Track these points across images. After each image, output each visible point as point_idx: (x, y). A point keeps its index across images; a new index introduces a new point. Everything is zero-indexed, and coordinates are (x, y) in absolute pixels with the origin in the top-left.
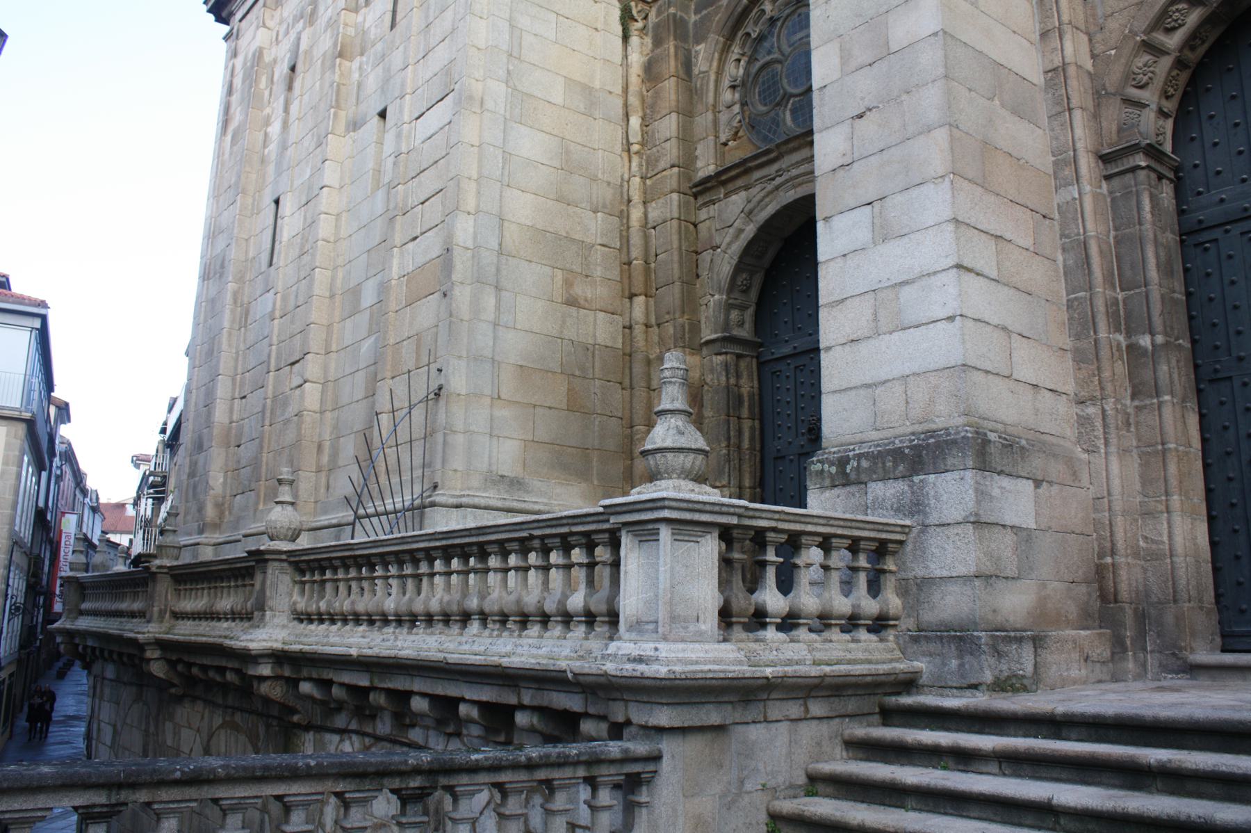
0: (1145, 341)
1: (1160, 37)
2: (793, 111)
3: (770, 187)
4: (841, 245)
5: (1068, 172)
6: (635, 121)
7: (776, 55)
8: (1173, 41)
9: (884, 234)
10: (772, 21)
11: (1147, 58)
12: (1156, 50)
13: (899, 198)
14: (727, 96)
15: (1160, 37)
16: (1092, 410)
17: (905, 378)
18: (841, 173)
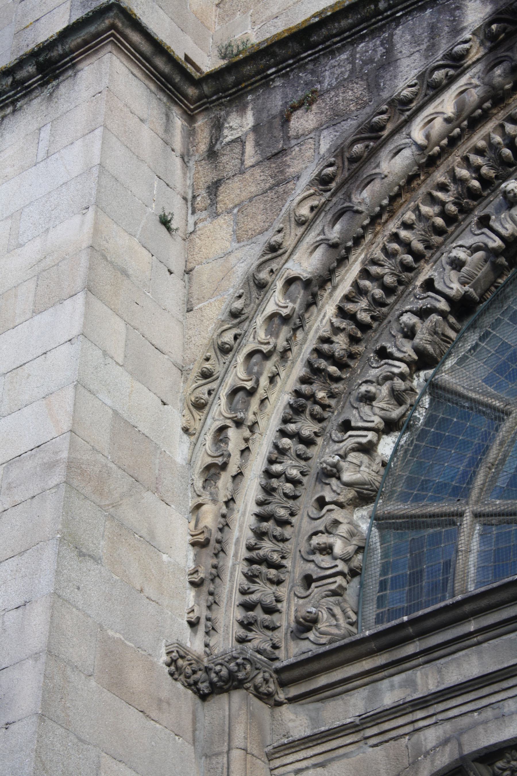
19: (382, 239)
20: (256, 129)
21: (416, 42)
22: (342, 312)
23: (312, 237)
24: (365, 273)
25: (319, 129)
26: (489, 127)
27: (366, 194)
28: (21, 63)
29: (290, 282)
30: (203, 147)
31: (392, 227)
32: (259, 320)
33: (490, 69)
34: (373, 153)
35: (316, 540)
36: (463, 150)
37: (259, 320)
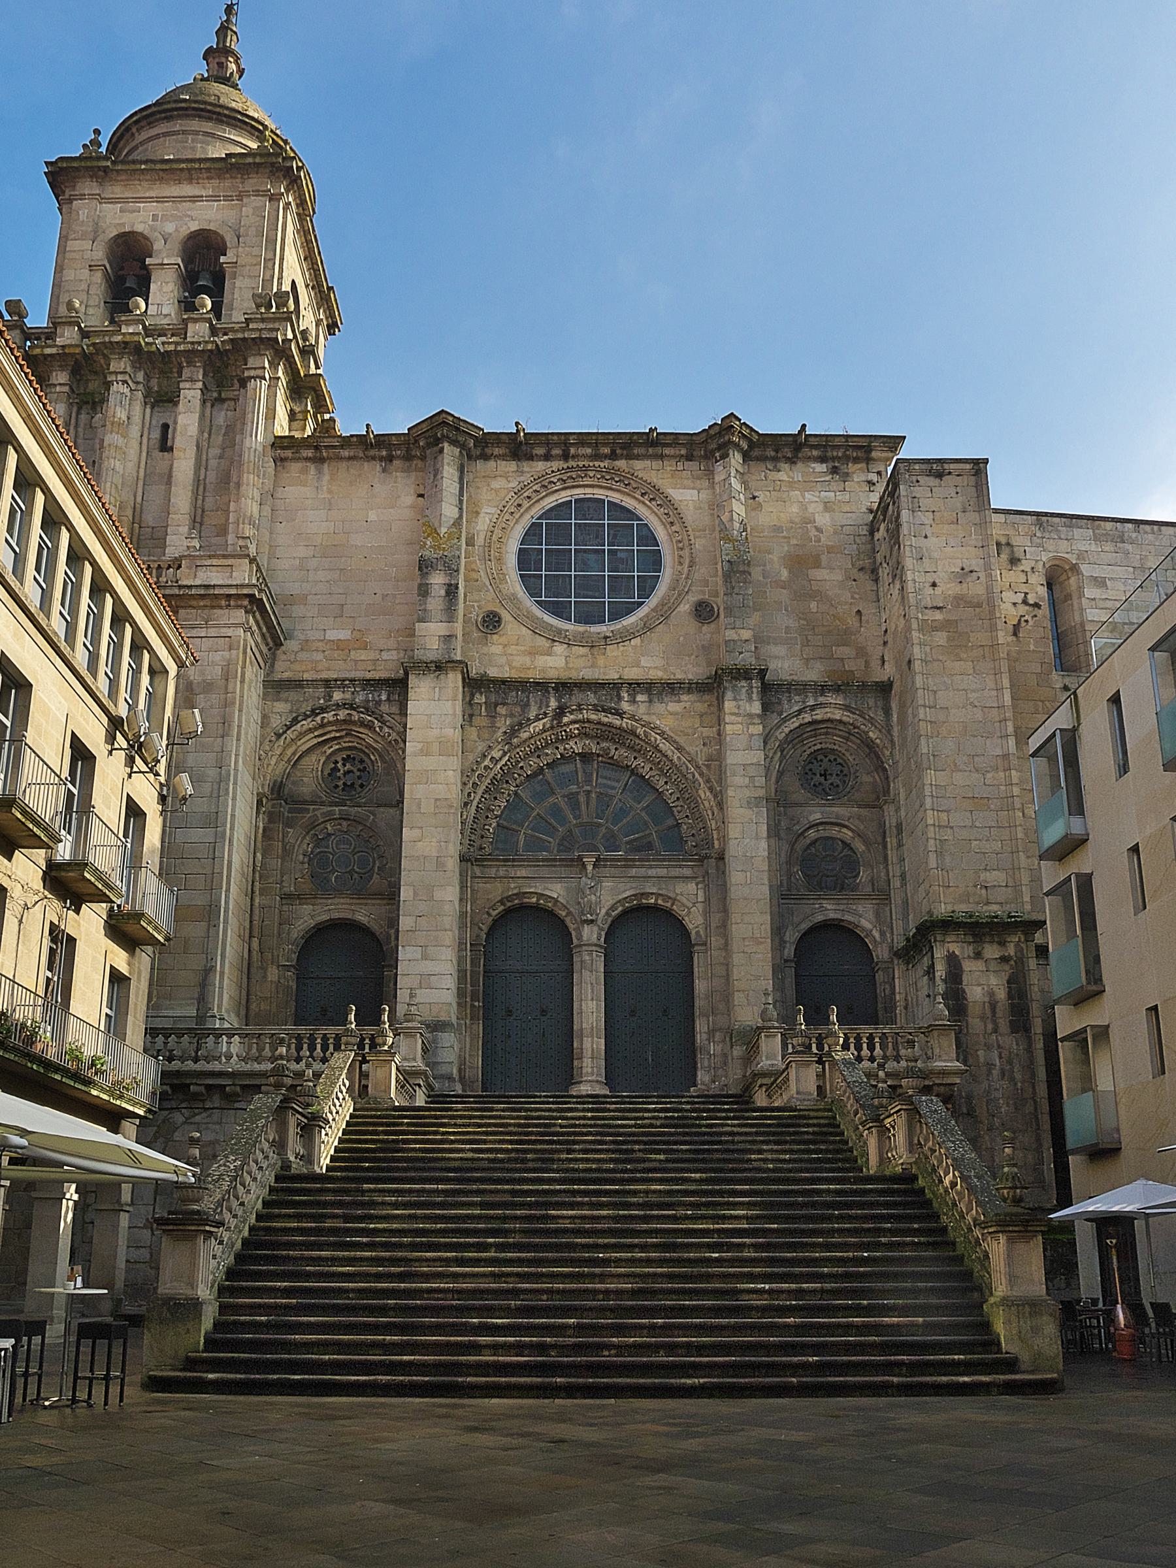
0: (476, 1004)
1: (491, 911)
2: (335, 878)
3: (326, 908)
4: (409, 956)
5: (464, 946)
6: (259, 855)
7: (331, 850)
8: (494, 913)
9: (425, 957)
10: (330, 835)
11: (486, 916)
12: (488, 913)
13: (432, 948)
14: (301, 857)
15: (491, 911)
16: (463, 1022)
17: (430, 1003)
18: (410, 933)
19: (515, 752)
20: (485, 703)
21: (536, 703)
22: (501, 768)
23: (499, 747)
24: (509, 760)
25: (506, 716)
26: (548, 733)
27: (515, 740)
28: (431, 662)
29: (492, 758)
30: (468, 699)
31: (518, 750)
32: (483, 765)
33: (552, 720)
34: (519, 729)
35: (487, 827)
36: (538, 738)
37: (483, 765)
